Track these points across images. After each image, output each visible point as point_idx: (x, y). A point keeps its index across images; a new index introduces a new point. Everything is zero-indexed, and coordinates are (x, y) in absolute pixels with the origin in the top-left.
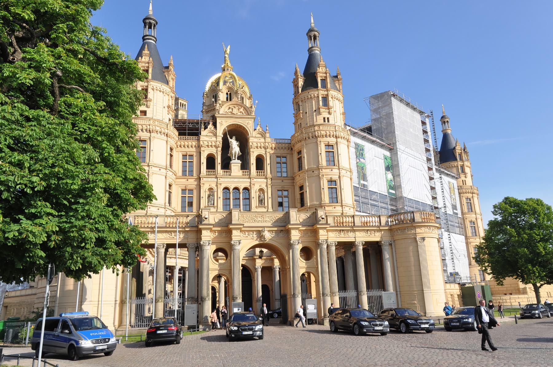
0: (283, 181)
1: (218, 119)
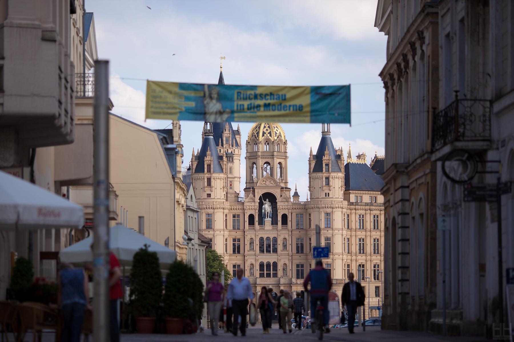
0: (300, 232)
1: (256, 189)
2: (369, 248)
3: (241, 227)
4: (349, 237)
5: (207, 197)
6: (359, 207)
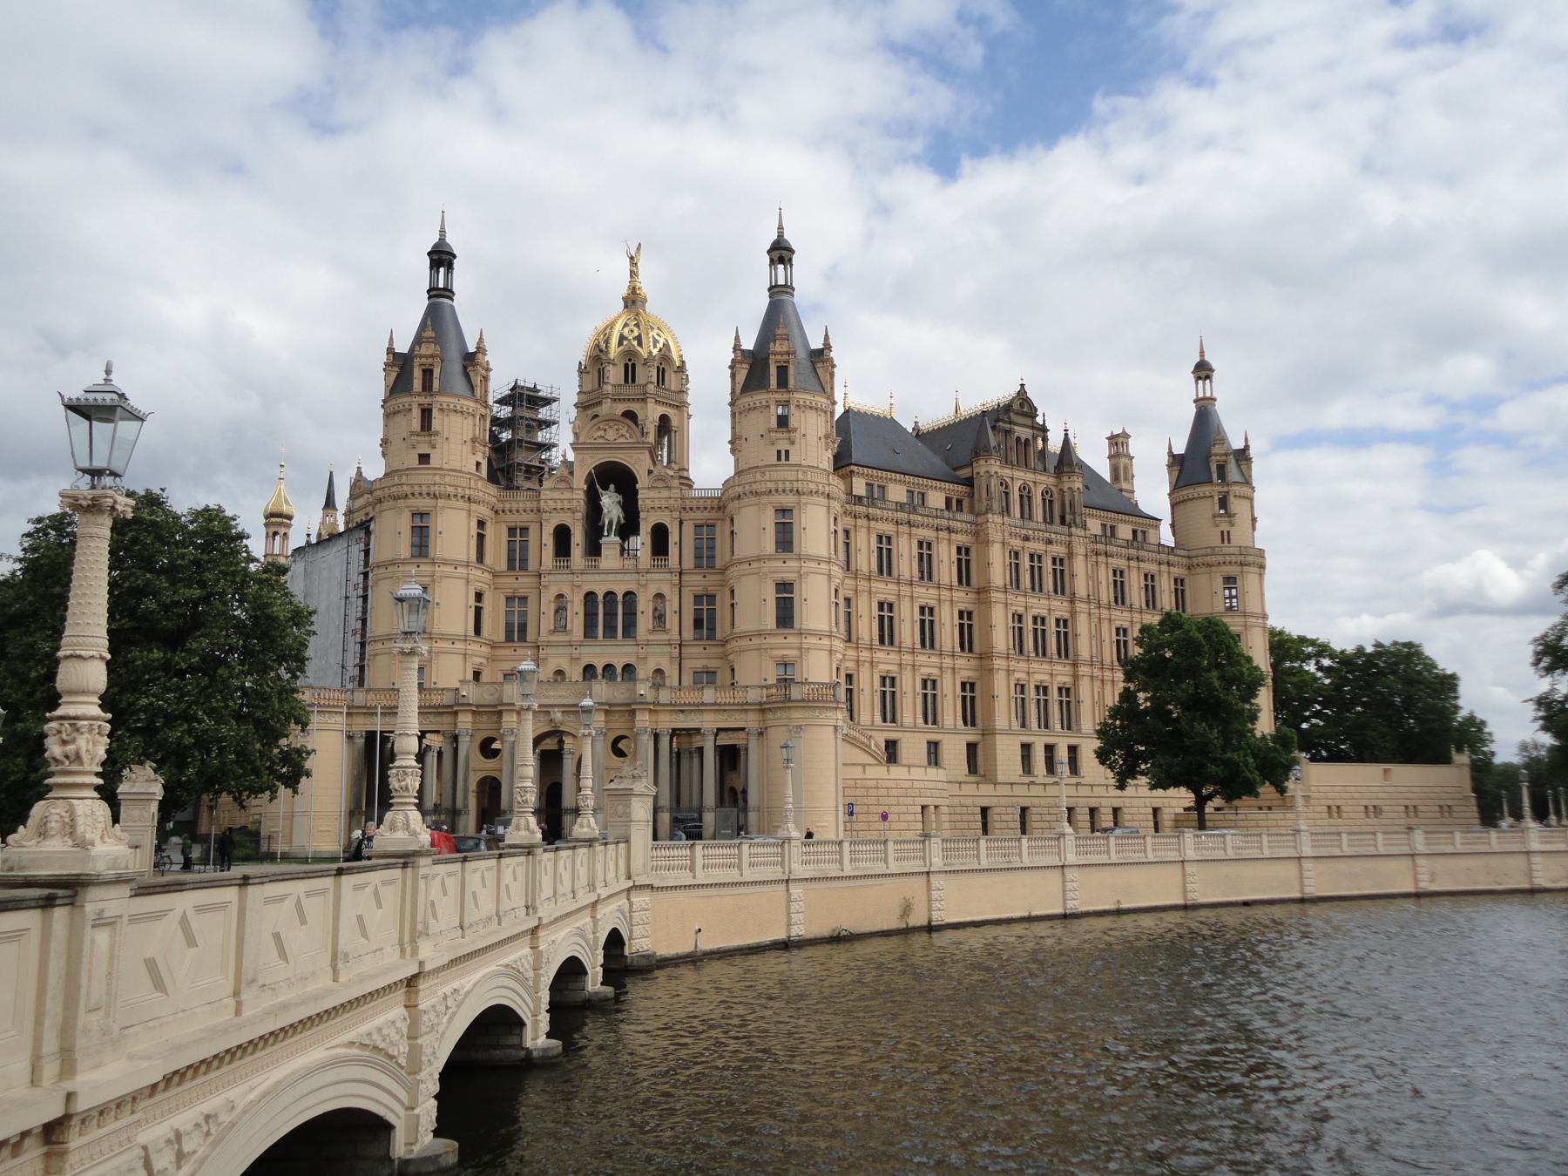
0: (704, 577)
2: (907, 631)
3: (532, 564)
4: (850, 594)
5: (420, 464)
6: (879, 512)
